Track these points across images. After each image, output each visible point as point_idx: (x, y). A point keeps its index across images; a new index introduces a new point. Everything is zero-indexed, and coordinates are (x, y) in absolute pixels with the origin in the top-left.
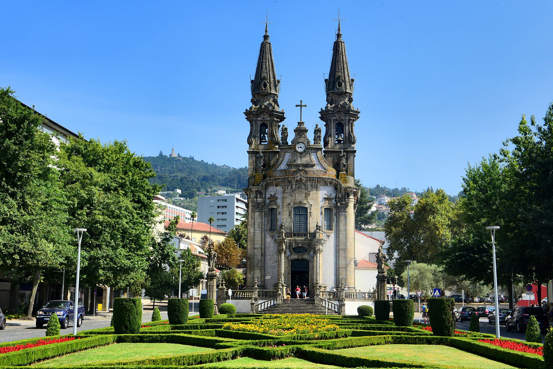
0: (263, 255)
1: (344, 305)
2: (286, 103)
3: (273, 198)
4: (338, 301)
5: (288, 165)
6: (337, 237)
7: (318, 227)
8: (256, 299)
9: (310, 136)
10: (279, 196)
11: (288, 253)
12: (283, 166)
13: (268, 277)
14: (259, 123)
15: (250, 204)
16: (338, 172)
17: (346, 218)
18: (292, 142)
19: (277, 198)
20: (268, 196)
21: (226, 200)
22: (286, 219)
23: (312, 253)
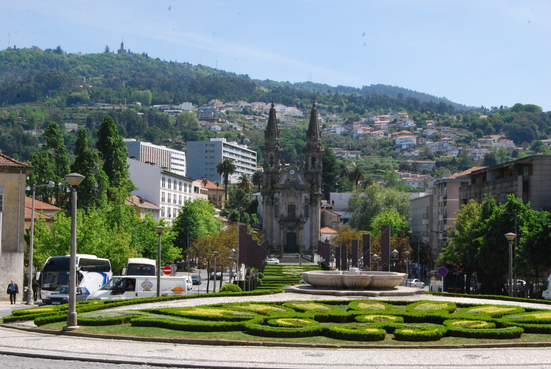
0: (272, 230)
1: (313, 257)
3: (277, 199)
6: (311, 220)
7: (301, 216)
10: (280, 198)
11: (285, 229)
13: (274, 242)
15: (264, 203)
16: (312, 184)
21: (213, 146)
23: (297, 229)
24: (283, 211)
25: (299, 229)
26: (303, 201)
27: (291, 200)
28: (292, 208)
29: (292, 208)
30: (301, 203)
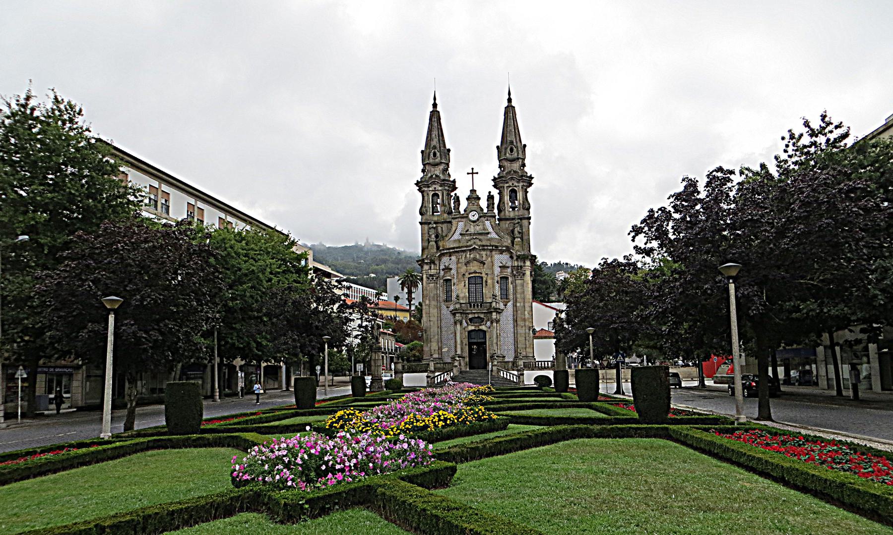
2: (457, 172)
3: (448, 269)
4: (518, 371)
5: (461, 234)
8: (433, 372)
9: (483, 203)
11: (465, 324)
12: (457, 236)
14: (431, 194)
17: (523, 285)
18: (465, 211)
19: (451, 269)
20: (442, 267)
22: (460, 290)
24: (460, 290)
25: (492, 323)
26: (497, 270)
27: (474, 267)
28: (476, 281)
29: (476, 281)
30: (493, 273)
